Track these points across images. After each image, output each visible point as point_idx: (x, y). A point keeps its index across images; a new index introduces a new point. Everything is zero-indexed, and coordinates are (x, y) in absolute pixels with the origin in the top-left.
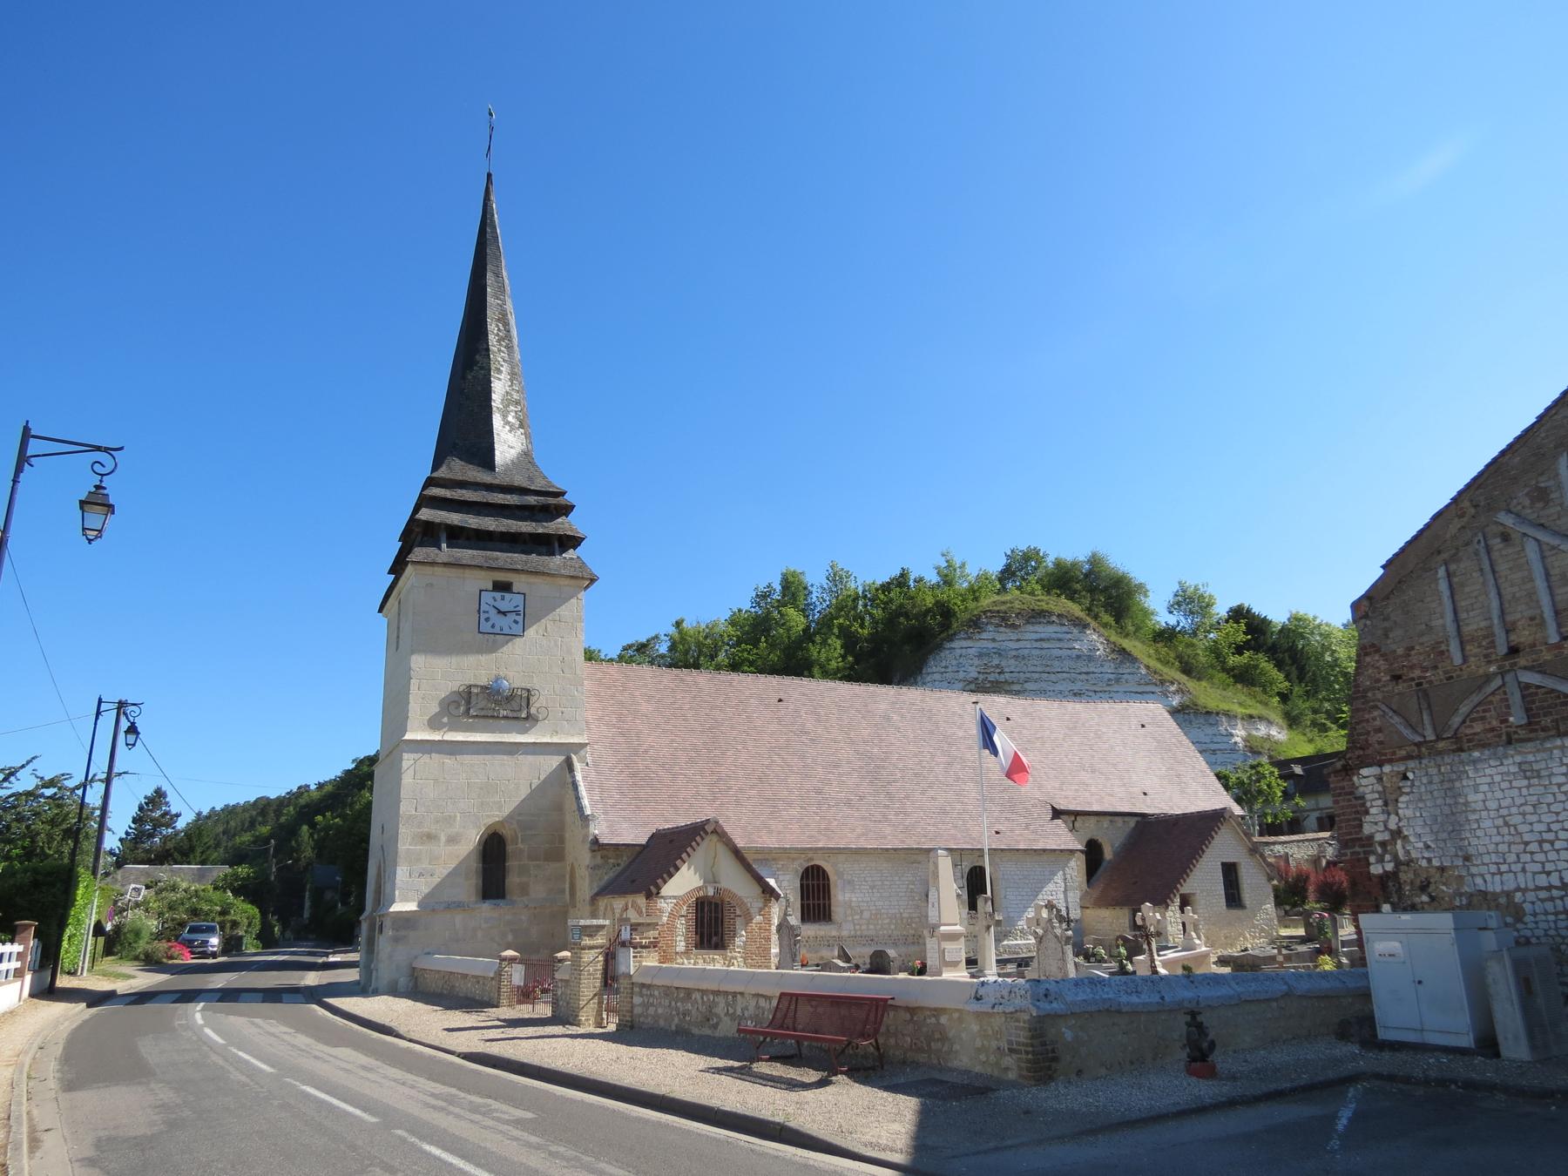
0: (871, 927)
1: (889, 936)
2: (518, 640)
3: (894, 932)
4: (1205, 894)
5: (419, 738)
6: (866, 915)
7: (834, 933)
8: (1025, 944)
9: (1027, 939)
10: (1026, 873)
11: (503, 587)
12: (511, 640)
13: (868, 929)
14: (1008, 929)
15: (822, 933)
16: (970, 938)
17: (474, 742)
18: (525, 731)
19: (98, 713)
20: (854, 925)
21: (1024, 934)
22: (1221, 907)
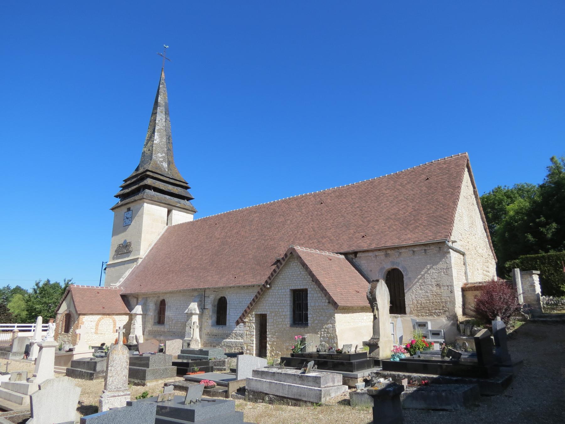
0: (175, 328)
1: (180, 332)
2: (130, 226)
3: (183, 331)
4: (273, 314)
5: (111, 263)
6: (174, 322)
7: (163, 330)
8: (234, 342)
9: (237, 339)
10: (241, 300)
11: (129, 209)
12: (129, 227)
13: (174, 328)
14: (229, 332)
15: (159, 329)
16: (211, 336)
17: (130, 260)
18: (128, 257)
19: (103, 265)
20: (169, 326)
21: (236, 336)
22: (286, 325)
